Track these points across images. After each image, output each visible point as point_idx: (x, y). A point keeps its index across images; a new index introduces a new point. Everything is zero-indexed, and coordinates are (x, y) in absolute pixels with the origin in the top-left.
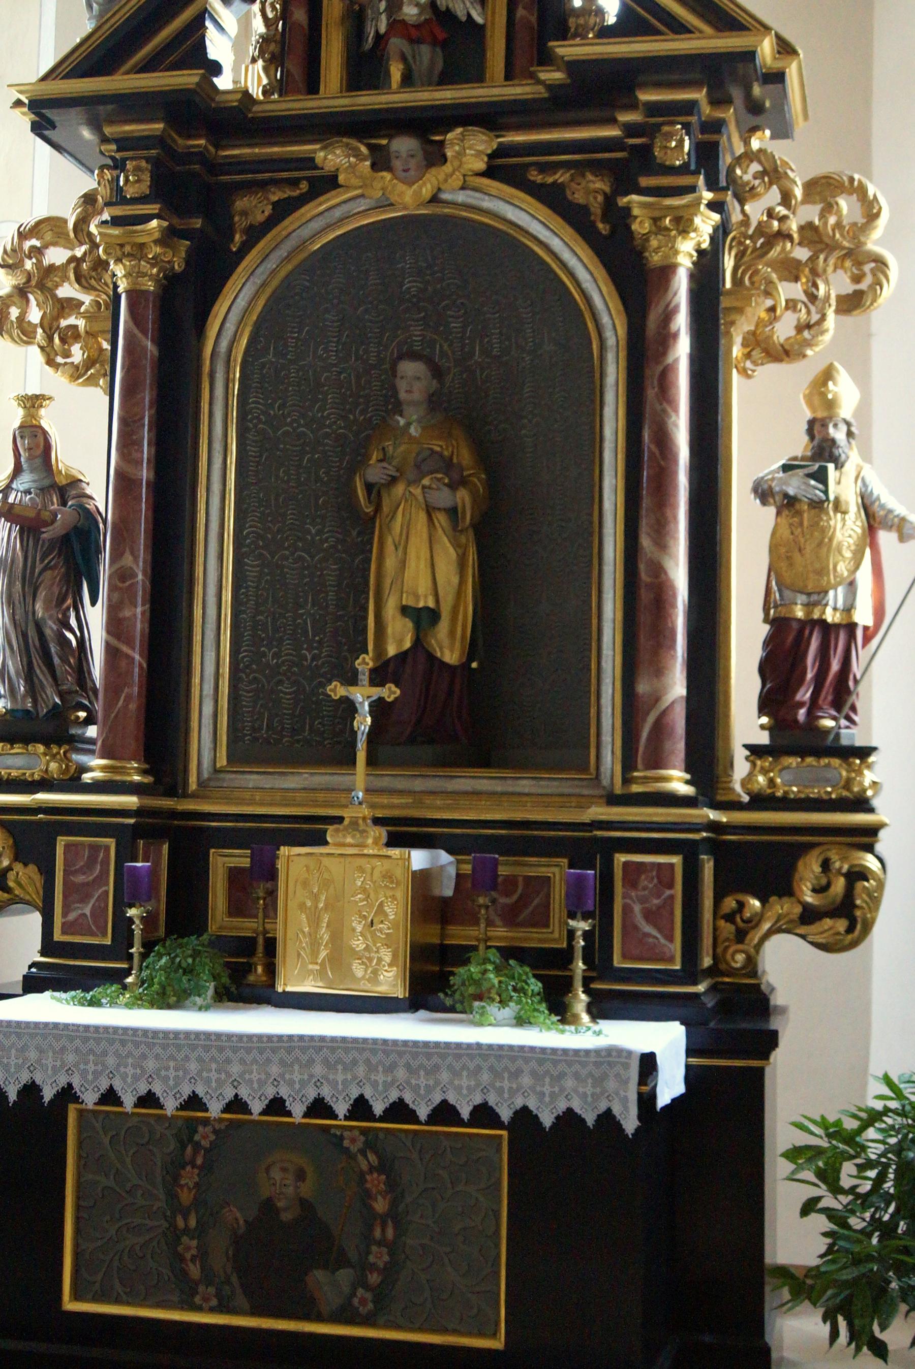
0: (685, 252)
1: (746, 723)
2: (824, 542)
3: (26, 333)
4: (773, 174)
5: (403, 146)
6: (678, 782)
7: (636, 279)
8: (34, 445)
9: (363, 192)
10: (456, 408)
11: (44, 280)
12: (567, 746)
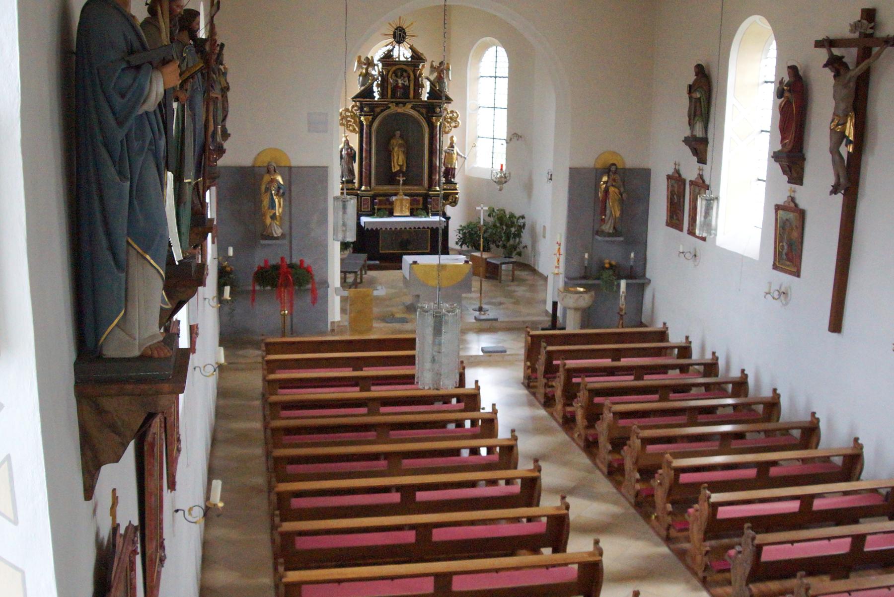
0: (438, 124)
2: (452, 158)
3: (343, 125)
4: (446, 109)
5: (401, 105)
6: (438, 188)
7: (432, 127)
9: (393, 109)
10: (401, 137)
12: (420, 184)
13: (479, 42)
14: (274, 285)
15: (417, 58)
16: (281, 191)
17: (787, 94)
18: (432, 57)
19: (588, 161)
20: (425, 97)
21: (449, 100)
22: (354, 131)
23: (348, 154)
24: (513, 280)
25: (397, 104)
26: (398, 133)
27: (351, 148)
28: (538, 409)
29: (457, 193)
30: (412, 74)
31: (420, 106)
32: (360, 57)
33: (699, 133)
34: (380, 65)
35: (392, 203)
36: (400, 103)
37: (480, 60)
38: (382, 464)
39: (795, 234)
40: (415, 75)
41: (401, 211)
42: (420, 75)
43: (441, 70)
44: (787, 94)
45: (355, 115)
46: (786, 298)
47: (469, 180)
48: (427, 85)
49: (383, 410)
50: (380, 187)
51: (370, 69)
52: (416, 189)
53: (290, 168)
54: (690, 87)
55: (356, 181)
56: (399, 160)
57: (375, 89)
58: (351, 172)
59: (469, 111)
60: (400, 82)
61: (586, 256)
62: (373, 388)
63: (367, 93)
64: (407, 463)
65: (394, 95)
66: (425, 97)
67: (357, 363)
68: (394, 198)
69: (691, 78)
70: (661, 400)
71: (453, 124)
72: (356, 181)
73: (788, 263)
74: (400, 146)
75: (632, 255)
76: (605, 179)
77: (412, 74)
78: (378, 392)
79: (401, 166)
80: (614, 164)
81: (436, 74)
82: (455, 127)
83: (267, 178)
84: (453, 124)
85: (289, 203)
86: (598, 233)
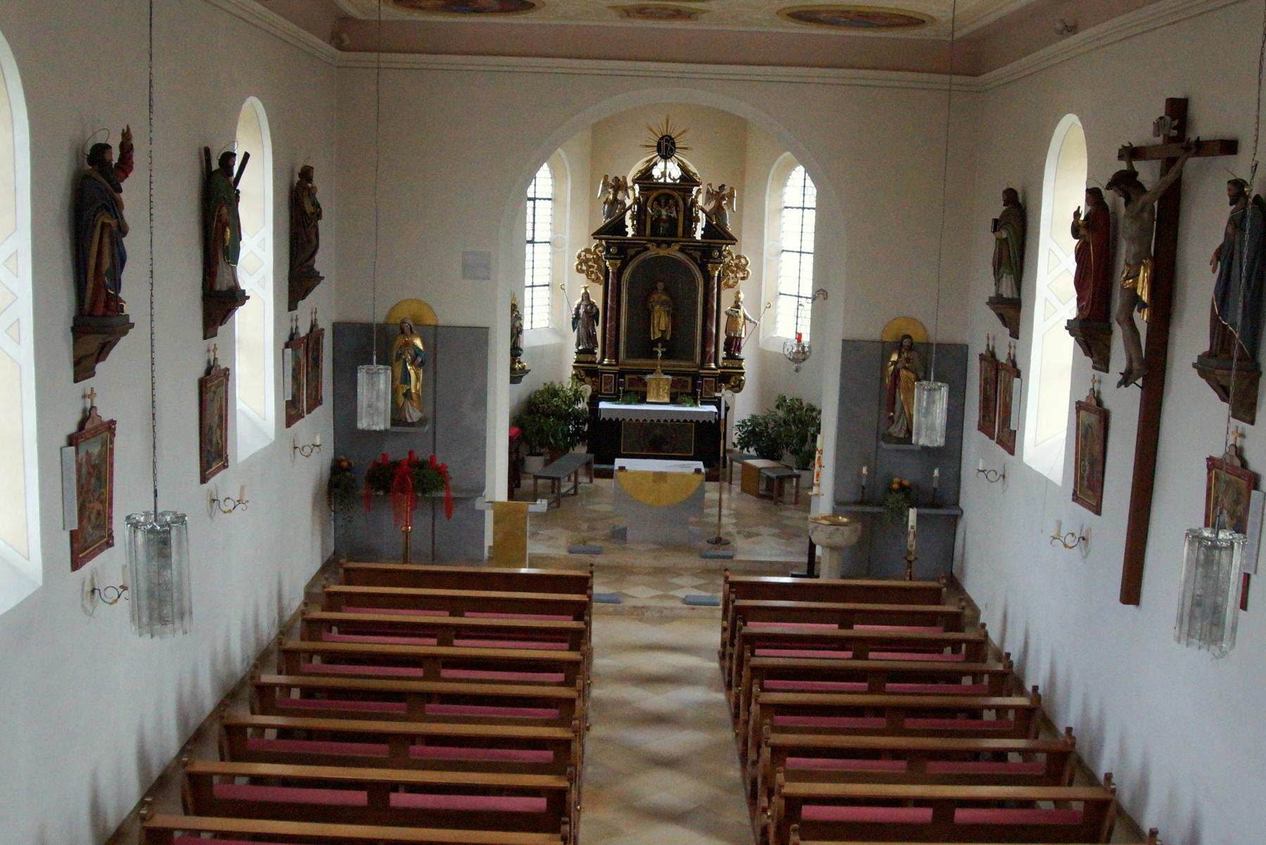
1: (722, 354)
2: (737, 323)
4: (730, 253)
5: (664, 246)
6: (713, 366)
7: (708, 278)
8: (586, 296)
9: (654, 251)
10: (667, 290)
11: (586, 261)
12: (691, 357)
13: (781, 158)
14: (387, 491)
15: (688, 179)
16: (419, 359)
17: (1083, 232)
18: (708, 178)
19: (871, 330)
20: (698, 235)
21: (732, 240)
22: (597, 280)
23: (586, 312)
24: (796, 502)
25: (659, 244)
26: (660, 285)
27: (592, 305)
28: (716, 691)
29: (742, 374)
30: (681, 203)
31: (689, 247)
32: (606, 177)
33: (1007, 292)
34: (637, 187)
35: (645, 385)
36: (663, 242)
37: (784, 185)
38: (382, 750)
39: (1097, 449)
40: (685, 204)
41: (658, 396)
42: (694, 203)
43: (719, 196)
44: (1083, 232)
45: (599, 258)
46: (1086, 546)
47: (764, 358)
48: (702, 216)
49: (446, 673)
50: (631, 361)
51: (620, 196)
52: (683, 365)
53: (436, 327)
54: (996, 221)
55: (598, 351)
56: (661, 323)
57: (628, 222)
58: (591, 338)
59: (766, 256)
60: (664, 212)
61: (864, 470)
62: (456, 642)
63: (615, 227)
64: (418, 749)
65: (654, 232)
66: (698, 235)
67: (456, 606)
68: (649, 376)
69: (998, 209)
70: (871, 691)
71: (740, 275)
72: (598, 351)
73: (1090, 493)
74: (662, 303)
75: (936, 472)
76: (894, 357)
77: (681, 203)
78: (464, 648)
79: (663, 332)
80: (909, 337)
81: (713, 203)
82: (743, 278)
83: (400, 340)
84: (740, 275)
85: (432, 378)
86: (888, 438)
